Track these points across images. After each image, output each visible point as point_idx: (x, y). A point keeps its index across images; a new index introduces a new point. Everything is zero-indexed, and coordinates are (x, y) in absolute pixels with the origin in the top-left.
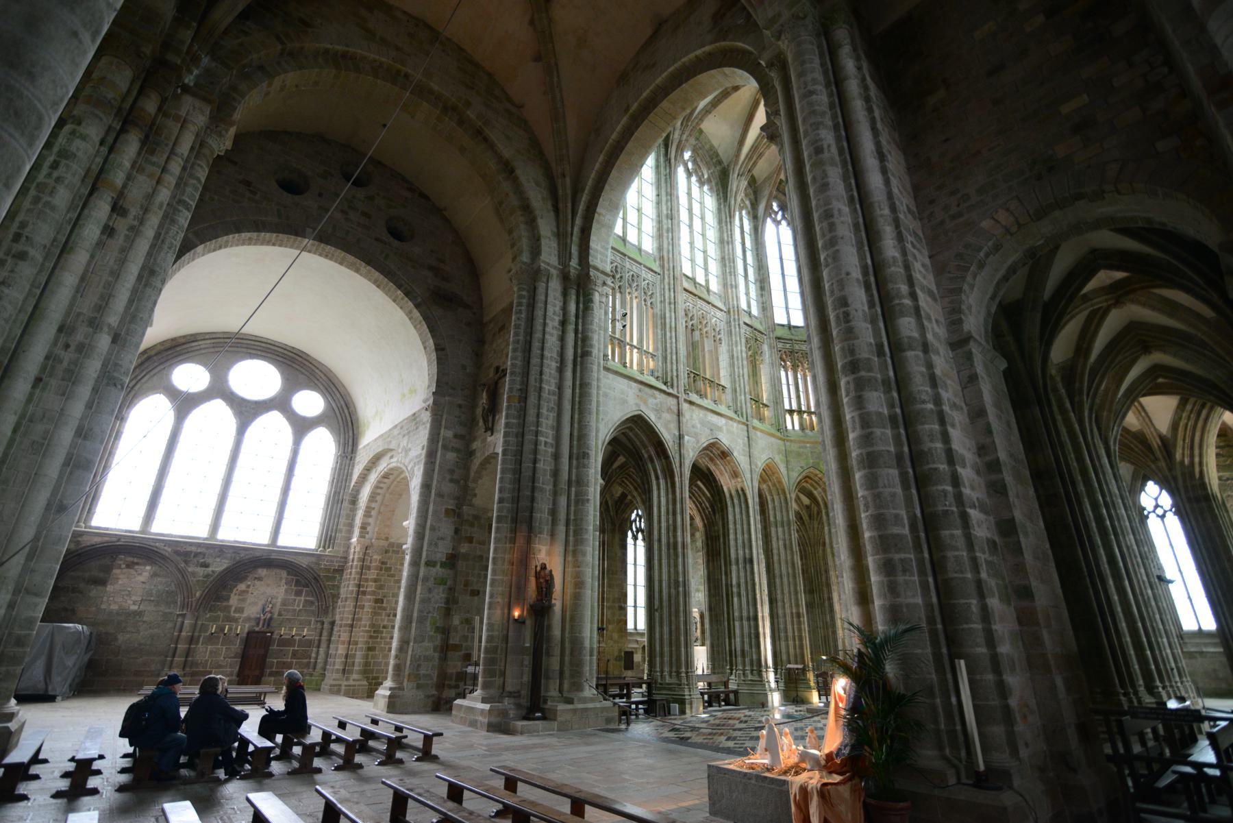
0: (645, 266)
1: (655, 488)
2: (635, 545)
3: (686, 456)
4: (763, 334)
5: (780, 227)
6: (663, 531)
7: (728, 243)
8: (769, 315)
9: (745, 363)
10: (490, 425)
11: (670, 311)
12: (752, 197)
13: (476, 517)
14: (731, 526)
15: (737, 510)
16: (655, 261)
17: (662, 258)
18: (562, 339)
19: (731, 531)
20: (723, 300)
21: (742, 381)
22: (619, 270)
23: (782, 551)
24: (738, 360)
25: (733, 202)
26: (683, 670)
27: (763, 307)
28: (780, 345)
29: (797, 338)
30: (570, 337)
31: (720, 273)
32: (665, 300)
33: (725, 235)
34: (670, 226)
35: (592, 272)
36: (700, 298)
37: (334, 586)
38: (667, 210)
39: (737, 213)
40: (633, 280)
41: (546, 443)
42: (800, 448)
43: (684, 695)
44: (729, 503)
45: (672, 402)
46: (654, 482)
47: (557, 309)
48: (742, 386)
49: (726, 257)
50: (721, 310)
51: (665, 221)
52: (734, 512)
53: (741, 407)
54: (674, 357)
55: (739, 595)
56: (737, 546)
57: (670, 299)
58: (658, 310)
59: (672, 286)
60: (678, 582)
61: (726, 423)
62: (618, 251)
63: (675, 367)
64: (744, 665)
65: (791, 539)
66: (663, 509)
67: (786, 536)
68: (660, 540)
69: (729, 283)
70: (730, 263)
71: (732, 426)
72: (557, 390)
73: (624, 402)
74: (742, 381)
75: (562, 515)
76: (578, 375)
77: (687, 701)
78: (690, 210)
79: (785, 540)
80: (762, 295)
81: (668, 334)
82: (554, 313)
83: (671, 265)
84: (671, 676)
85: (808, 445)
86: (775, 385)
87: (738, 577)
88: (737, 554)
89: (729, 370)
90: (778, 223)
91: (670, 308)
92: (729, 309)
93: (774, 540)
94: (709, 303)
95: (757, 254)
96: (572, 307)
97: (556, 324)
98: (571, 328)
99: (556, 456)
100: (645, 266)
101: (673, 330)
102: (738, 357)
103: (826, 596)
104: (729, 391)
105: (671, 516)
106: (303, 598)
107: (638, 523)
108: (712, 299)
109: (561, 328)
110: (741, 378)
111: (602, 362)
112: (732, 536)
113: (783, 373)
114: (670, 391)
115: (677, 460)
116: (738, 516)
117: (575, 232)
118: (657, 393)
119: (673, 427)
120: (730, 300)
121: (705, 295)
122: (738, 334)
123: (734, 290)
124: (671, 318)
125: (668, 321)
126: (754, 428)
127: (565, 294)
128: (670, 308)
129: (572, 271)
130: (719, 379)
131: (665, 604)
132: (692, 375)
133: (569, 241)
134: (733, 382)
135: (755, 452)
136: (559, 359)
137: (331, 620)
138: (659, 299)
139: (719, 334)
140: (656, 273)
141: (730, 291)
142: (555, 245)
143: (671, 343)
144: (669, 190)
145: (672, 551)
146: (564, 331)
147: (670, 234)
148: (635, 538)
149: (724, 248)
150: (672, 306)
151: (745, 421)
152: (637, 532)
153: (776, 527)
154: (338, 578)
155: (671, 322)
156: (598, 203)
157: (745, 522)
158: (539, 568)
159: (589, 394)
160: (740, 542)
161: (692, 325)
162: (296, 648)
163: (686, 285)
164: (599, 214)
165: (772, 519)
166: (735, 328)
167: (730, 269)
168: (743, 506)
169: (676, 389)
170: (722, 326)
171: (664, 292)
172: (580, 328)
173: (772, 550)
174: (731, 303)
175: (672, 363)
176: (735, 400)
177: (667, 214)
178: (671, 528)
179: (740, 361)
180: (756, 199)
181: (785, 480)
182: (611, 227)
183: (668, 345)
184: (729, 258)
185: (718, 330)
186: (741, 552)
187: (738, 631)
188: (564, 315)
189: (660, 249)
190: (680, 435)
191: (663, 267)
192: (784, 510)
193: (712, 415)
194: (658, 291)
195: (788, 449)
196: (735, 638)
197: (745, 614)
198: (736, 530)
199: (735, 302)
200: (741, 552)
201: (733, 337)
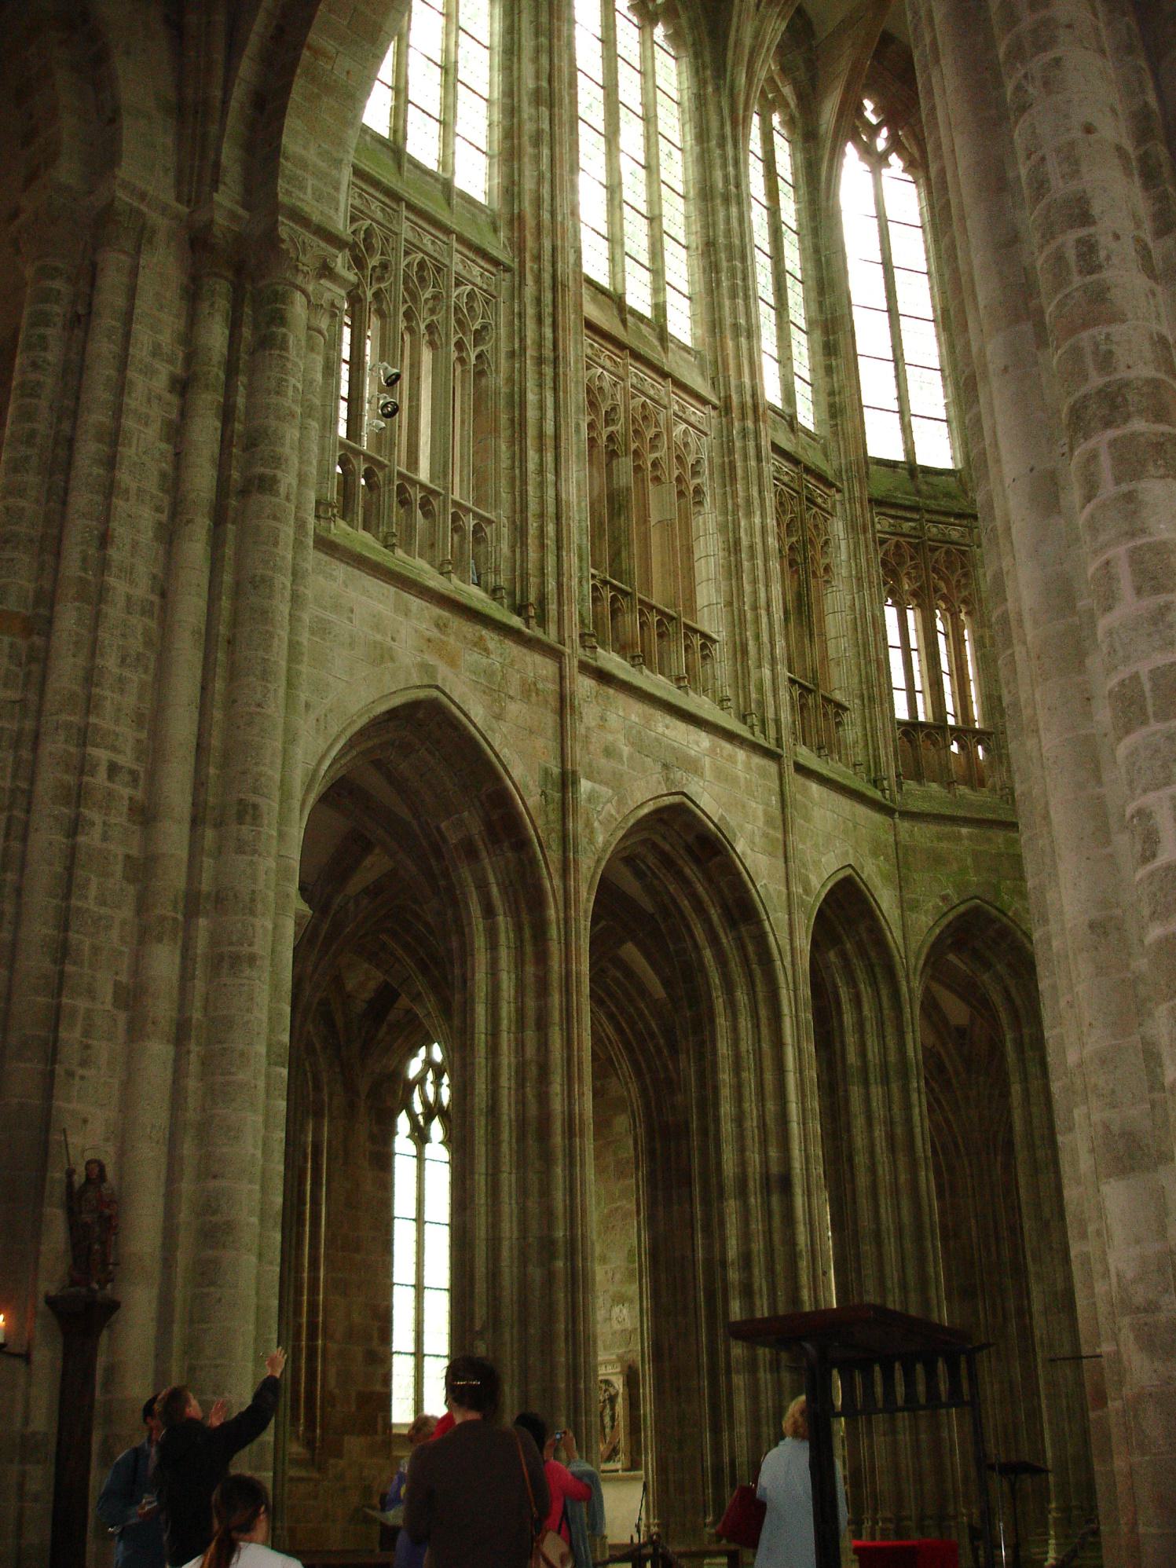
0: (461, 239)
1: (480, 942)
2: (420, 1158)
3: (583, 841)
4: (830, 485)
5: (885, 172)
7: (726, 199)
8: (849, 428)
9: (775, 566)
11: (540, 386)
12: (802, 75)
14: (725, 1077)
15: (745, 1023)
16: (495, 230)
17: (516, 221)
18: (177, 432)
19: (726, 1092)
20: (709, 373)
21: (764, 620)
22: (377, 243)
23: (882, 1156)
24: (752, 557)
25: (742, 79)
27: (832, 406)
28: (883, 524)
30: (205, 431)
31: (700, 287)
32: (523, 348)
33: (718, 175)
34: (546, 126)
35: (286, 228)
36: (637, 356)
38: (537, 78)
39: (756, 120)
40: (422, 279)
41: (113, 769)
42: (940, 839)
44: (719, 1004)
45: (541, 667)
46: (478, 924)
47: (166, 338)
48: (765, 638)
49: (721, 240)
50: (704, 401)
51: (527, 110)
52: (735, 1029)
53: (761, 704)
54: (551, 528)
56: (741, 1137)
57: (540, 346)
58: (498, 380)
59: (548, 310)
60: (552, 1242)
61: (712, 750)
62: (376, 184)
63: (551, 560)
65: (908, 1120)
66: (506, 1010)
67: (896, 1110)
68: (493, 1110)
69: (728, 321)
70: (730, 259)
71: (732, 759)
72: (155, 598)
73: (382, 655)
74: (764, 620)
76: (229, 551)
78: (610, 88)
79: (890, 1123)
80: (829, 370)
81: (532, 455)
82: (156, 351)
83: (547, 244)
85: (964, 831)
87: (746, 1236)
88: (743, 1164)
89: (723, 586)
90: (877, 161)
91: (541, 374)
92: (728, 398)
93: (859, 1123)
94: (665, 375)
95: (817, 250)
96: (216, 336)
97: (160, 383)
98: (207, 401)
100: (461, 239)
101: (549, 443)
102: (751, 547)
103: (1011, 1305)
104: (722, 652)
105: (530, 1034)
107: (430, 1089)
108: (672, 362)
109: (174, 399)
110: (763, 612)
111: (311, 521)
112: (726, 1108)
113: (891, 614)
114: (536, 632)
115: (554, 855)
116: (746, 1044)
117: (234, 104)
118: (491, 639)
120: (732, 372)
121: (654, 354)
122: (754, 477)
123: (743, 340)
124: (541, 407)
125: (531, 414)
126: (800, 769)
127: (193, 294)
128: (541, 374)
129: (220, 219)
130: (691, 609)
131: (509, 1312)
132: (608, 594)
133: (214, 129)
134: (738, 623)
135: (803, 846)
136: (166, 500)
138: (504, 348)
139: (695, 473)
140: (496, 263)
141: (730, 344)
142: (169, 141)
143: (541, 485)
144: (544, 19)
146: (184, 414)
147: (546, 151)
148: (420, 1137)
149: (714, 212)
150: (548, 370)
151: (771, 745)
152: (429, 1119)
153: (866, 1083)
155: (541, 420)
156: (312, 17)
157: (768, 1063)
159: (265, 615)
160: (751, 1123)
161: (611, 438)
163: (591, 311)
164: (317, 52)
165: (852, 1058)
166: (745, 458)
167: (734, 276)
168: (763, 1013)
169: (552, 628)
170: (704, 448)
171: (522, 325)
172: (241, 401)
173: (851, 1159)
174: (733, 382)
175: (542, 546)
176: (741, 677)
177: (537, 91)
178: (533, 1071)
179: (760, 562)
180: (813, 79)
181: (894, 935)
182: (355, 96)
183: (531, 490)
184: (730, 247)
185: (691, 460)
186: (754, 1158)
187: (741, 1404)
188: (190, 358)
189: (510, 190)
191: (519, 248)
192: (889, 1030)
193: (669, 719)
194: (502, 320)
195: (904, 836)
196: (731, 1428)
198: (738, 1088)
199: (746, 380)
200: (754, 1158)
201: (739, 487)
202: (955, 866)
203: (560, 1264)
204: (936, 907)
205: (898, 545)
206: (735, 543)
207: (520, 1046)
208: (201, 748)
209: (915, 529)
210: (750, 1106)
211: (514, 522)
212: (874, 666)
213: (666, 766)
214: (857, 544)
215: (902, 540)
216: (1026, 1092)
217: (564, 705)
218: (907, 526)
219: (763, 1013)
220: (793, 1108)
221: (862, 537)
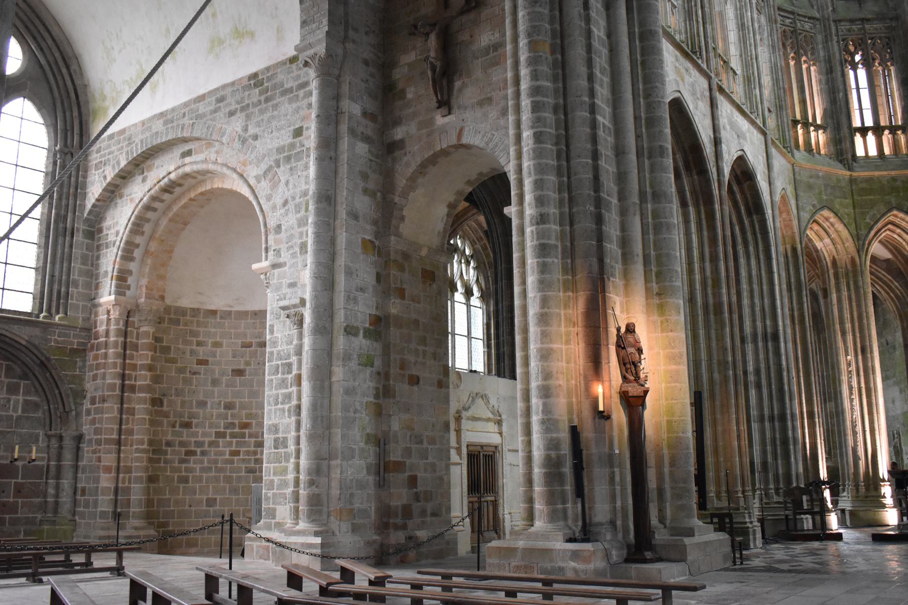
6: (698, 286)
10: (446, 97)
13: (406, 256)
15: (753, 262)
26: (740, 488)
29: (800, 13)
37: (74, 376)
43: (746, 523)
55: (758, 386)
64: (767, 482)
66: (696, 253)
75: (638, 248)
77: (751, 530)
79: (792, 310)
84: (719, 497)
86: (777, 80)
99: (619, 152)
105: (707, 264)
106: (21, 398)
116: (754, 273)
119: (708, 122)
137: (75, 433)
145: (712, 316)
154: (79, 364)
158: (623, 330)
160: (758, 309)
162: (20, 480)
178: (710, 282)
186: (759, 324)
190: (715, 138)
192: (791, 268)
197: (766, 412)
198: (751, 291)
200: (759, 324)
202: (817, 191)
203: (731, 372)
204: (811, 210)
205: (784, 31)
206: (742, 25)
207: (703, 270)
208: (637, 118)
209: (791, 23)
210: (757, 301)
211: (684, 8)
212: (782, 91)
213: (738, 136)
214: (772, 30)
215: (787, 28)
216: (839, 300)
217: (713, 105)
218: (788, 21)
219: (762, 257)
220: (778, 302)
221: (774, 26)
